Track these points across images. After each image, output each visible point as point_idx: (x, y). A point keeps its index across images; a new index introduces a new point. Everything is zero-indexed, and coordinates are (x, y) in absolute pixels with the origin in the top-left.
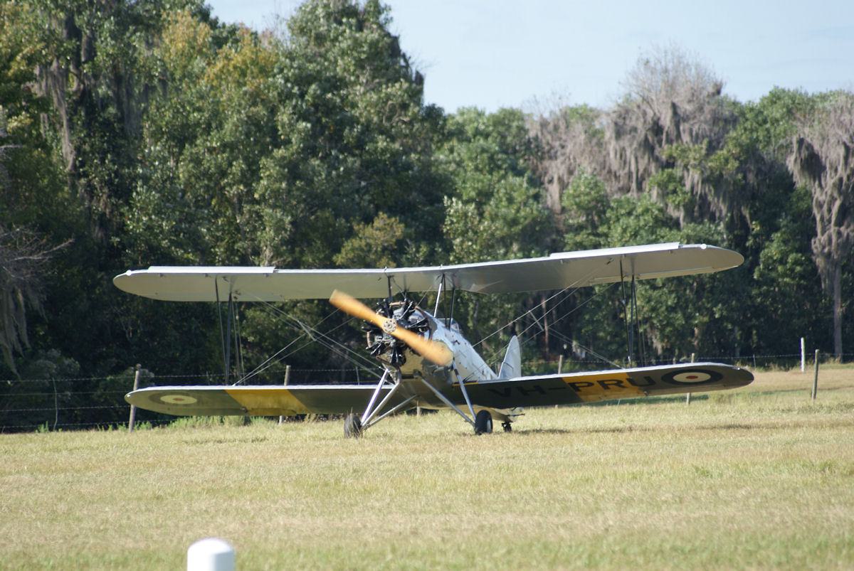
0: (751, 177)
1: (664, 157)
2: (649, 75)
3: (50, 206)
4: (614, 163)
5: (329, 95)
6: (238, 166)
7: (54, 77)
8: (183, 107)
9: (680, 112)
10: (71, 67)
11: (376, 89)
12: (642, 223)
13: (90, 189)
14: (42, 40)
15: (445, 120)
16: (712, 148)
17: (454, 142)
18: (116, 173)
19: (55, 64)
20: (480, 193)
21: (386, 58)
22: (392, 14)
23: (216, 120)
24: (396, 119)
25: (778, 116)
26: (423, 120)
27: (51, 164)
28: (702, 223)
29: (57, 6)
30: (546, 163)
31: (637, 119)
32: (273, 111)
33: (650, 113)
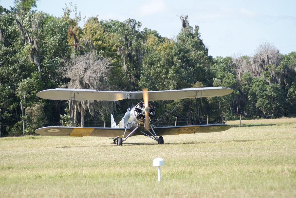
0: (286, 72)
1: (265, 68)
2: (262, 49)
3: (121, 80)
4: (254, 70)
6: (164, 71)
7: (122, 50)
10: (126, 48)
11: (196, 52)
12: (260, 83)
13: (130, 76)
15: (213, 59)
16: (277, 66)
17: (215, 64)
18: (136, 72)
19: (122, 47)
20: (221, 76)
21: (199, 45)
22: (200, 35)
23: (159, 60)
24: (201, 59)
25: (292, 58)
27: (121, 71)
28: (274, 83)
29: (123, 34)
30: (237, 69)
31: (259, 59)
32: (173, 58)
33: (262, 57)
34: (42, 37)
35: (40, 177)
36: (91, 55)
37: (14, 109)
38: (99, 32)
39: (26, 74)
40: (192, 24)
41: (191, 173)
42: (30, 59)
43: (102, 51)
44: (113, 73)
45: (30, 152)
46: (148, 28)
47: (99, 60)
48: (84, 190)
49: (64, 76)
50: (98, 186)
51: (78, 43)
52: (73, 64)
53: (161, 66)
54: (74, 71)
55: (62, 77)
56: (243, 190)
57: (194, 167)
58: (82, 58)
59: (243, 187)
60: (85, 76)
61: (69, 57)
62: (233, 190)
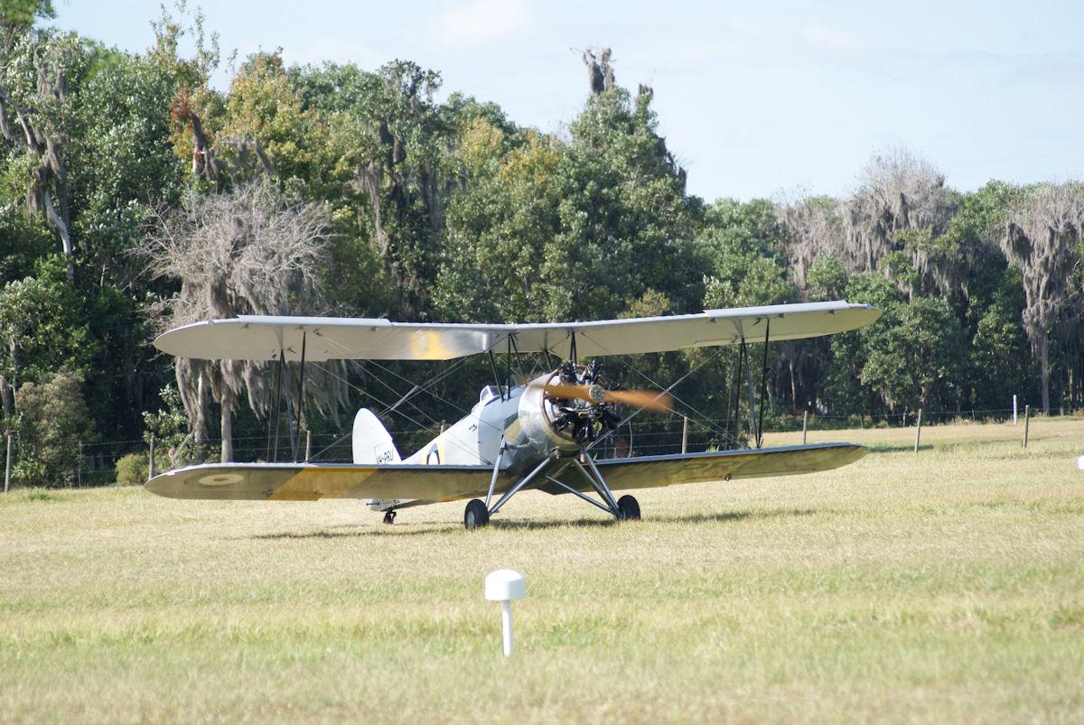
0: (970, 257)
1: (895, 240)
3: (368, 286)
5: (605, 191)
6: (526, 251)
7: (371, 177)
8: (480, 200)
9: (908, 201)
10: (385, 167)
11: (643, 184)
13: (401, 269)
14: (361, 145)
15: (705, 209)
16: (936, 233)
17: (712, 228)
18: (423, 256)
20: (735, 272)
21: (654, 158)
22: (657, 119)
23: (506, 213)
24: (662, 208)
26: (686, 208)
28: (927, 296)
30: (792, 246)
31: (871, 208)
32: (556, 204)
33: (881, 200)
34: (76, 128)
35: (67, 639)
36: (256, 194)
38: (286, 108)
39: (15, 260)
40: (626, 78)
41: (622, 625)
42: (31, 207)
43: (299, 177)
44: (337, 259)
45: (31, 549)
46: (466, 96)
47: (287, 213)
48: (231, 688)
49: (159, 272)
50: (284, 675)
51: (207, 148)
52: (189, 228)
53: (514, 234)
54: (194, 251)
55: (149, 274)
56: (812, 688)
57: (635, 601)
58: (223, 203)
59: (814, 674)
60: (237, 270)
61: (175, 201)
62: (776, 688)
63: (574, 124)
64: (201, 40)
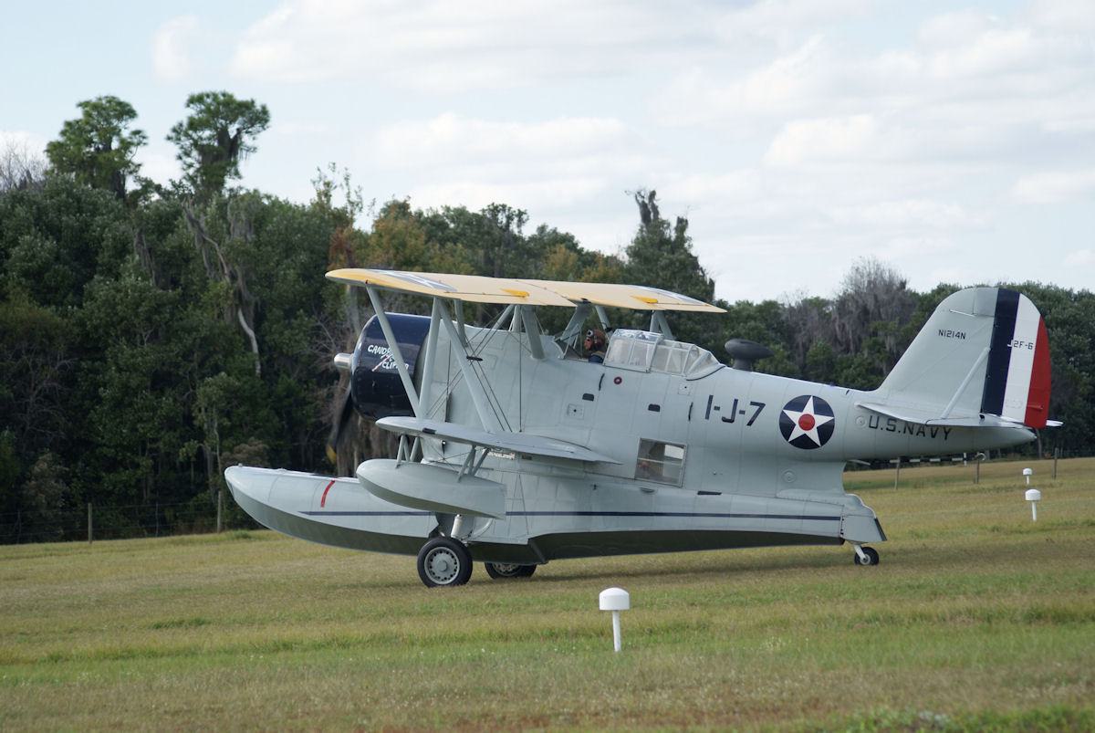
9: (879, 298)
22: (692, 242)
37: (189, 458)
40: (668, 214)
49: (322, 367)
63: (630, 248)
64: (349, 193)
